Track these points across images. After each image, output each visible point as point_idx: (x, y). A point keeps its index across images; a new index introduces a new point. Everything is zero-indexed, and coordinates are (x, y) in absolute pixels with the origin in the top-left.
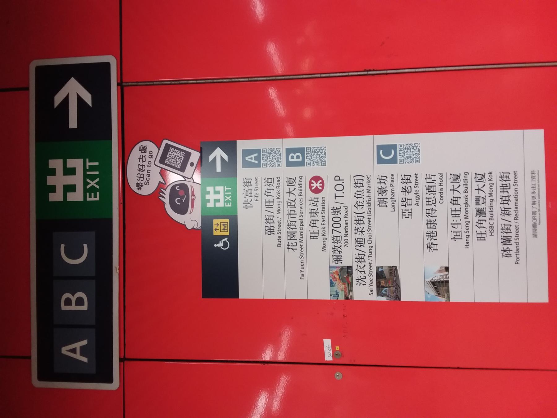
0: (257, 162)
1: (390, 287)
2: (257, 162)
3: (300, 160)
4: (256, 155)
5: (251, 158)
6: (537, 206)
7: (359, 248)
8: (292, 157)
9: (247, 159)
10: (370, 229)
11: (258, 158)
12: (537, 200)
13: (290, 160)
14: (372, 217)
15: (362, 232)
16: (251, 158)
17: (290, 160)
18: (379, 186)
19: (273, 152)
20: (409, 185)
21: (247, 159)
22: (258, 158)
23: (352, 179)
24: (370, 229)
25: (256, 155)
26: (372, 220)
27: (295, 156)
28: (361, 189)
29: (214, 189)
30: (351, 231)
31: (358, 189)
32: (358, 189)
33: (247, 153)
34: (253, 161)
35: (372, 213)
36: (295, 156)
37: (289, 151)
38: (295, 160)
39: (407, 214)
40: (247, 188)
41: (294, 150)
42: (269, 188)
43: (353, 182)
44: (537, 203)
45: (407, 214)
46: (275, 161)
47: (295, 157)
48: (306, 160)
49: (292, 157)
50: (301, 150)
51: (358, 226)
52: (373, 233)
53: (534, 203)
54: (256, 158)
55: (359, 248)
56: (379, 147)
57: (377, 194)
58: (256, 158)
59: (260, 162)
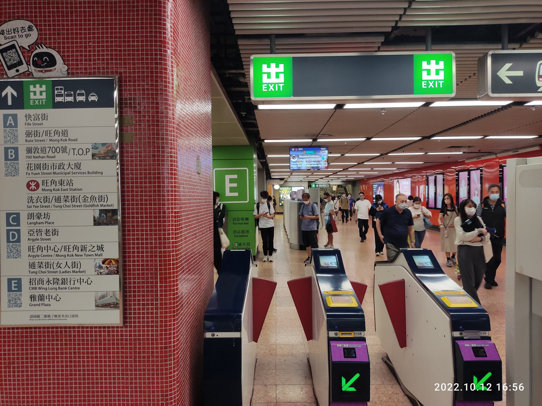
0: (8, 125)
1: (106, 219)
2: (8, 125)
3: (10, 158)
4: (13, 125)
5: (10, 121)
6: (54, 318)
7: (54, 199)
8: (11, 152)
9: (10, 117)
10: (74, 206)
11: (10, 126)
12: (58, 318)
13: (9, 150)
14: (83, 208)
15: (66, 201)
16: (10, 121)
17: (9, 150)
18: (43, 214)
19: (16, 137)
20: (51, 234)
21: (10, 117)
22: (10, 126)
23: (105, 194)
24: (74, 206)
25: (13, 125)
26: (81, 208)
27: (12, 154)
28: (97, 200)
29: (44, 91)
30: (66, 193)
31: (97, 199)
32: (97, 199)
33: (15, 117)
34: (9, 122)
35: (85, 208)
36: (12, 154)
37: (16, 149)
38: (10, 154)
39: (31, 232)
40: (40, 117)
41: (16, 153)
42: (61, 133)
43: (103, 194)
44: (56, 318)
45: (31, 232)
46: (8, 139)
47: (11, 153)
48: (9, 162)
49: (11, 152)
50: (16, 158)
51: (70, 198)
52: (71, 208)
53: (55, 316)
54: (10, 124)
55: (54, 199)
56: (18, 214)
57: (37, 212)
58: (10, 124)
59: (8, 127)
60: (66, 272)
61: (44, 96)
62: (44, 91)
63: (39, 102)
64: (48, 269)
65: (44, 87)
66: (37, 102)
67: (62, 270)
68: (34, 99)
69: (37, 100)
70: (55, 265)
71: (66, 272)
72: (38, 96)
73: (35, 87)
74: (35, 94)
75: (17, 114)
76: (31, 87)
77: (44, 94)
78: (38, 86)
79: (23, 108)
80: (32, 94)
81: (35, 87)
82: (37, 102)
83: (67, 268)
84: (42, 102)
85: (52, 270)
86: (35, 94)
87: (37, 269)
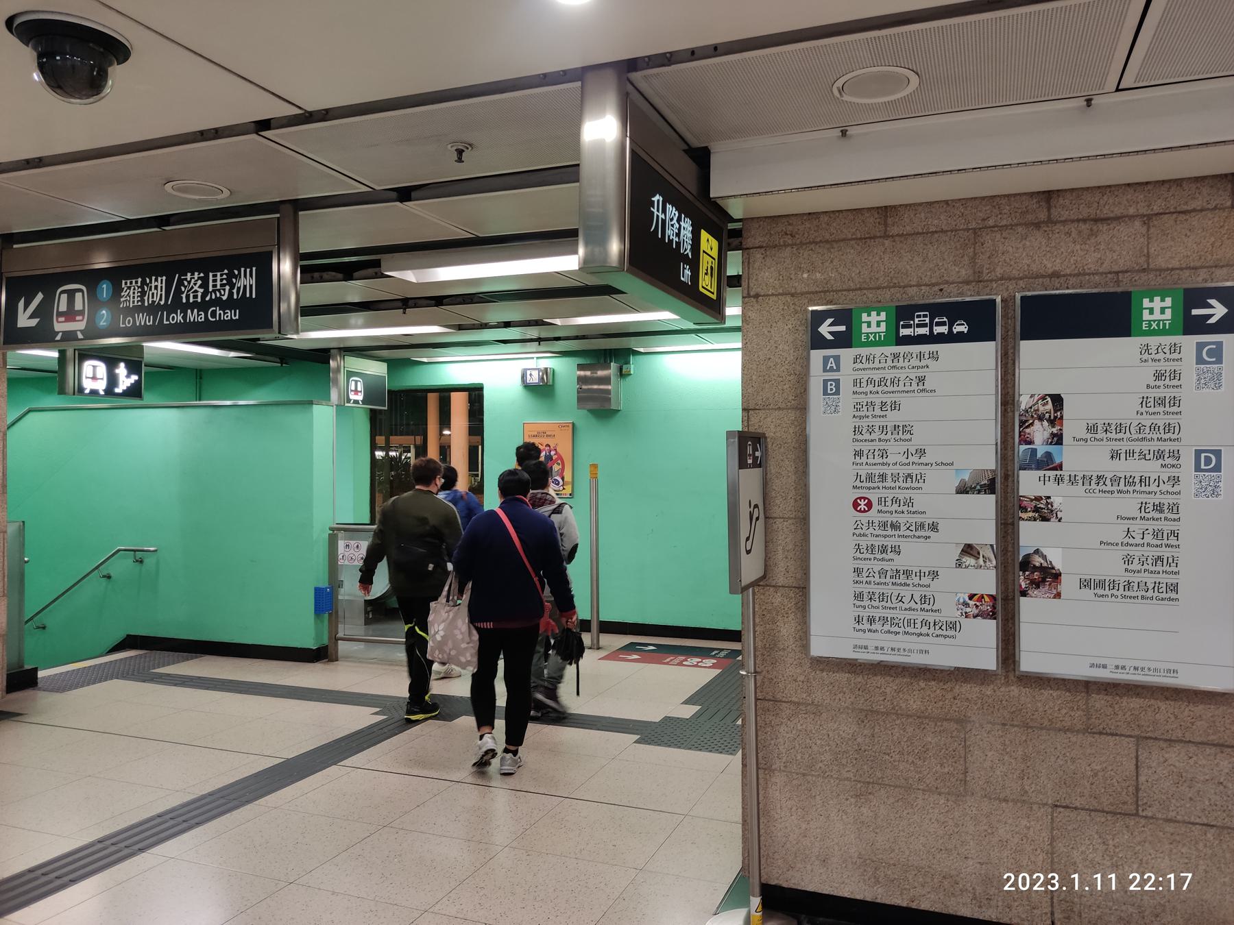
60: (910, 609)
64: (884, 603)
65: (883, 314)
66: (871, 337)
67: (904, 606)
70: (894, 599)
71: (910, 609)
72: (874, 329)
73: (869, 315)
74: (869, 326)
76: (864, 317)
77: (883, 325)
79: (850, 346)
80: (864, 326)
81: (869, 315)
82: (871, 337)
83: (912, 604)
85: (889, 604)
86: (869, 326)
87: (866, 603)
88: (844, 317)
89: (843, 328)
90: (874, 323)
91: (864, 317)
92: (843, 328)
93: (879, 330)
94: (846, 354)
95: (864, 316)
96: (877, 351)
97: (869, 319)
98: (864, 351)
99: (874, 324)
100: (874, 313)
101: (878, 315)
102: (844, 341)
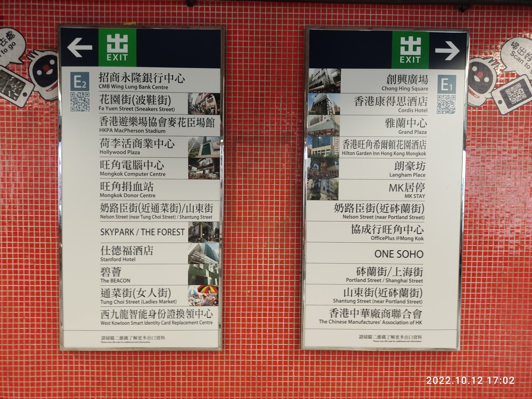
33: (85, 77)
61: (125, 49)
62: (125, 43)
63: (118, 57)
66: (115, 57)
68: (112, 54)
69: (115, 54)
73: (113, 37)
74: (113, 45)
75: (88, 73)
76: (109, 37)
78: (117, 36)
80: (109, 46)
81: (113, 37)
82: (115, 57)
84: (123, 57)
88: (91, 36)
89: (90, 48)
90: (118, 44)
91: (109, 38)
92: (90, 48)
93: (121, 51)
94: (94, 72)
95: (109, 37)
96: (121, 70)
97: (112, 40)
98: (111, 70)
99: (117, 45)
100: (117, 36)
101: (121, 37)
102: (91, 59)
